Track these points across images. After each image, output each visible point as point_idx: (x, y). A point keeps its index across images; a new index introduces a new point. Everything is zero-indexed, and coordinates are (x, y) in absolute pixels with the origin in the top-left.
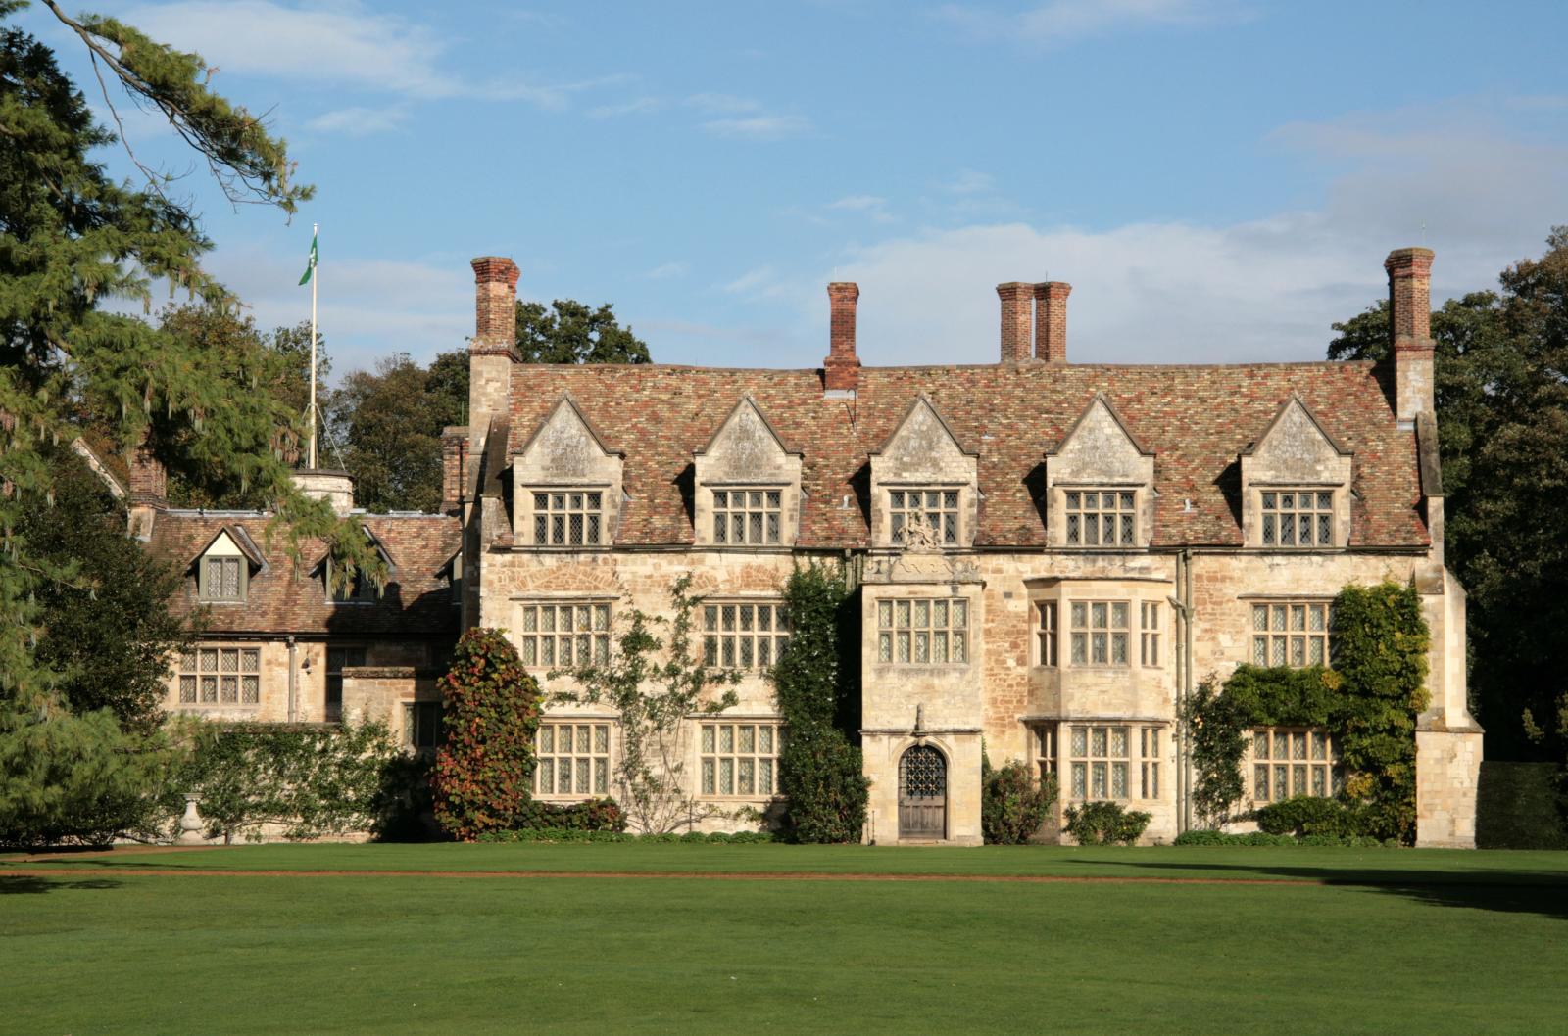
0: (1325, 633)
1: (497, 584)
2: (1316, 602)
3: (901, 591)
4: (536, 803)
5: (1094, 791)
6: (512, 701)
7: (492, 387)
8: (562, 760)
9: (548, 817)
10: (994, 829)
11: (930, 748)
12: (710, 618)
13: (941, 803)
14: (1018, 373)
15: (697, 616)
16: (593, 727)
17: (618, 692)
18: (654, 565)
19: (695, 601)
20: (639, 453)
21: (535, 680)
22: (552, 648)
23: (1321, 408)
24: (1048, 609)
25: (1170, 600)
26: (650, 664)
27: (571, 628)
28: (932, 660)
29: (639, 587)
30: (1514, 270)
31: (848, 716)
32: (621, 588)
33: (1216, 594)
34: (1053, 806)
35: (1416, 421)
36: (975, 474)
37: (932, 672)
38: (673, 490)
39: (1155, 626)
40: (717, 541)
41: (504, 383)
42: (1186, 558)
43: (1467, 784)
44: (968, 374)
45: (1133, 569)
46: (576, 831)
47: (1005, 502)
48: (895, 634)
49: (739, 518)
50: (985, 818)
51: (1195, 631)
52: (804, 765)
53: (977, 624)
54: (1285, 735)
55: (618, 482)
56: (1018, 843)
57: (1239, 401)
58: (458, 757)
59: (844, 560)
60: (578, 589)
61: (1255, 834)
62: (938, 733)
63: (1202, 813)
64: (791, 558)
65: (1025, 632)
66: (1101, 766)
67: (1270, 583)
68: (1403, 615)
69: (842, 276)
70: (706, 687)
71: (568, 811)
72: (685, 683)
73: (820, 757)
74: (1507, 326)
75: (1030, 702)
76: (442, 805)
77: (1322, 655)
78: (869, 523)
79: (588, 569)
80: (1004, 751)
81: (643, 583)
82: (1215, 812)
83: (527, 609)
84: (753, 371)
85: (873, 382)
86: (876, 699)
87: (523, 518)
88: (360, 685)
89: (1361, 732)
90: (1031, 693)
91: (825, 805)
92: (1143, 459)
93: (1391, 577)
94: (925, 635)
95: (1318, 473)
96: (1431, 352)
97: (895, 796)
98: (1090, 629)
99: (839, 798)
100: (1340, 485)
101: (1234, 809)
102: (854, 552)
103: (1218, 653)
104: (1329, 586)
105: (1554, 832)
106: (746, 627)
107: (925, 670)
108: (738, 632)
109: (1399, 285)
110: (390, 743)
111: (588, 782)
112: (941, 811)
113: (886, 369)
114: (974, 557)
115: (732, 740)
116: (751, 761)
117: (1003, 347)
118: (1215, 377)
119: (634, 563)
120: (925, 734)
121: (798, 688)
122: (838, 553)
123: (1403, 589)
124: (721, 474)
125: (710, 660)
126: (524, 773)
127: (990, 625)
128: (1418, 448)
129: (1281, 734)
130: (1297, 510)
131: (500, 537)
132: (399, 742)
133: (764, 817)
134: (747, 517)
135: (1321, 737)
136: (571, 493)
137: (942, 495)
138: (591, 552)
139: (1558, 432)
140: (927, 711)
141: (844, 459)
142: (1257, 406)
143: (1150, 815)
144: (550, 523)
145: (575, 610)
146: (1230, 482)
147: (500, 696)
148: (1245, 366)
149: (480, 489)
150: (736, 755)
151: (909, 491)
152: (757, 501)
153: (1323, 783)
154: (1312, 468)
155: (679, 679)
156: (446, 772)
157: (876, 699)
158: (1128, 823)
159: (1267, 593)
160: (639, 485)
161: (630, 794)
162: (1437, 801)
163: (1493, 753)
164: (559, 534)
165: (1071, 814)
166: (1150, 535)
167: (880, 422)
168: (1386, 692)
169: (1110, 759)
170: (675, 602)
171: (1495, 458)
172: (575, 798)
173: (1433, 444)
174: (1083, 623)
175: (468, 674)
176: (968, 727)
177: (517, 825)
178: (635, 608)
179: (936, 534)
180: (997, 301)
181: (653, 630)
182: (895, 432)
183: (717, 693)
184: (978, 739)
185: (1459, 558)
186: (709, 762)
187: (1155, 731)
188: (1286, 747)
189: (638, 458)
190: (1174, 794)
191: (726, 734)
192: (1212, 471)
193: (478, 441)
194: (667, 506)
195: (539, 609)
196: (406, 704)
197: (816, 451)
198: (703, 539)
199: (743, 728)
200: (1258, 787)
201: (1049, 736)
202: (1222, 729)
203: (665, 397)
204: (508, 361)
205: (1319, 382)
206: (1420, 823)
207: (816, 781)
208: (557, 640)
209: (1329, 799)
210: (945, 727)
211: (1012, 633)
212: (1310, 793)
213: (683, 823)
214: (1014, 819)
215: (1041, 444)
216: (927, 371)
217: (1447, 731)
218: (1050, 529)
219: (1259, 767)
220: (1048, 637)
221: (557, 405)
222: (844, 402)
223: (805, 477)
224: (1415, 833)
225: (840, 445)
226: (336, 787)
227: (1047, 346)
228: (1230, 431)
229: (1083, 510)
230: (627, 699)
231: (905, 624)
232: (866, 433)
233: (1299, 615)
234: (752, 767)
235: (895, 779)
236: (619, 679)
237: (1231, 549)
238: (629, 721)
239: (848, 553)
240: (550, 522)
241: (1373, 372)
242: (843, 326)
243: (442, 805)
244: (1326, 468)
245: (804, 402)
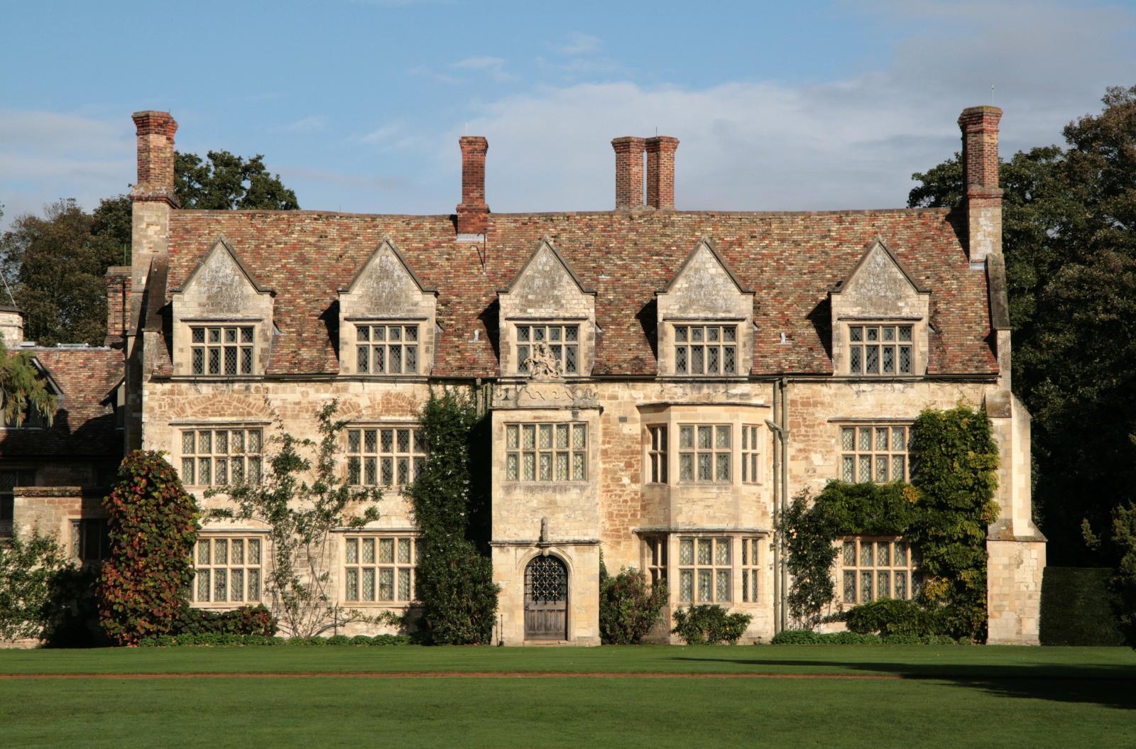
0: (906, 453)
1: (157, 411)
2: (897, 424)
3: (527, 416)
4: (194, 610)
5: (700, 595)
6: (171, 517)
7: (152, 230)
8: (217, 571)
9: (205, 623)
10: (611, 630)
11: (553, 557)
12: (354, 441)
13: (563, 607)
14: (631, 219)
15: (342, 439)
16: (246, 541)
17: (269, 508)
18: (302, 393)
19: (340, 425)
20: (288, 291)
21: (192, 498)
22: (209, 468)
23: (901, 250)
24: (659, 432)
25: (767, 423)
27: (226, 450)
28: (554, 478)
29: (289, 413)
30: (1077, 125)
31: (478, 528)
32: (272, 414)
33: (808, 418)
34: (663, 609)
35: (986, 262)
36: (593, 310)
38: (320, 325)
39: (754, 447)
40: (360, 371)
41: (163, 227)
42: (782, 386)
43: (1032, 587)
44: (586, 219)
45: (735, 395)
46: (231, 635)
47: (621, 336)
48: (521, 454)
49: (379, 350)
50: (602, 621)
51: (790, 452)
52: (439, 574)
53: (596, 444)
54: (870, 544)
55: (269, 317)
56: (632, 642)
57: (829, 244)
58: (121, 569)
59: (475, 388)
60: (232, 415)
61: (843, 634)
62: (560, 544)
63: (797, 615)
64: (427, 386)
65: (638, 453)
66: (706, 573)
67: (857, 408)
68: (975, 436)
69: (471, 131)
70: (350, 503)
71: (224, 617)
72: (331, 500)
73: (453, 567)
74: (1067, 176)
75: (643, 516)
76: (107, 613)
77: (903, 472)
78: (497, 354)
79: (242, 397)
80: (620, 560)
81: (292, 409)
82: (808, 614)
83: (185, 434)
84: (392, 216)
85: (501, 226)
86: (504, 513)
87: (181, 350)
88: (30, 503)
89: (938, 540)
90: (644, 508)
91: (458, 610)
92: (744, 297)
93: (964, 402)
94: (548, 456)
95: (899, 309)
96: (999, 200)
97: (521, 602)
98: (696, 450)
99: (471, 603)
100: (919, 320)
101: (825, 611)
102: (485, 381)
103: (812, 471)
105: (1109, 630)
106: (386, 449)
107: (548, 488)
108: (379, 454)
109: (971, 139)
110: (58, 556)
111: (242, 591)
112: (563, 615)
113: (513, 215)
114: (592, 385)
115: (373, 551)
116: (391, 570)
117: (618, 196)
118: (808, 223)
119: (284, 391)
120: (549, 545)
121: (434, 504)
122: (470, 381)
123: (975, 413)
124: (363, 310)
125: (354, 480)
126: (182, 583)
127: (607, 446)
128: (988, 286)
129: (867, 544)
130: (881, 342)
131: (160, 367)
132: (67, 556)
133: (402, 621)
134: (387, 349)
135: (903, 546)
136: (226, 327)
137: (564, 329)
138: (244, 381)
139: (1112, 271)
140: (550, 525)
141: (475, 296)
142: (845, 249)
143: (750, 617)
144: (207, 354)
145: (230, 434)
146: (821, 317)
147: (161, 512)
148: (834, 213)
149: (142, 324)
150: (378, 564)
151: (534, 326)
152: (396, 335)
153: (904, 587)
154: (894, 304)
155: (326, 496)
156: (110, 583)
157: (504, 513)
158: (730, 625)
160: (288, 320)
161: (281, 601)
162: (1005, 603)
163: (1054, 558)
164: (214, 365)
165: (679, 616)
166: (750, 365)
167: (507, 264)
168: (961, 505)
169: (714, 567)
170: (321, 427)
171: (1057, 295)
172: (230, 605)
173: (1002, 281)
174: (691, 444)
175: (130, 492)
176: (587, 538)
177: (176, 631)
178: (285, 432)
179: (558, 364)
180: (612, 154)
181: (302, 452)
182: (521, 272)
183: (360, 509)
184: (596, 549)
185: (1024, 386)
186: (352, 571)
187: (755, 541)
188: (871, 555)
189: (287, 296)
190: (772, 598)
191: (368, 546)
192: (805, 307)
193: (140, 280)
194: (314, 339)
195: (197, 433)
196: (73, 521)
197: (450, 289)
198: (347, 369)
199: (383, 540)
200: (846, 591)
201: (660, 546)
202: (814, 539)
203: (312, 240)
204: (167, 206)
205: (900, 227)
206: (991, 622)
207: (450, 588)
208: (213, 461)
209: (909, 602)
210: (566, 538)
211: (627, 453)
212: (893, 596)
213: (329, 627)
214: (628, 621)
215: (652, 283)
216: (549, 217)
217: (1014, 540)
218: (660, 360)
219: (847, 573)
220: (659, 457)
221: (213, 247)
222: (475, 245)
223: (439, 313)
224: (986, 631)
225: (471, 284)
226: (7, 598)
227: (658, 195)
228: (822, 271)
229: (690, 342)
230: (278, 515)
231: (530, 446)
232: (495, 273)
233: (883, 436)
234: (392, 576)
235: (522, 585)
236: (270, 497)
237: (822, 377)
238: (280, 535)
239: (479, 381)
240: (207, 354)
241: (948, 218)
242: (473, 176)
243: (107, 613)
244: (907, 304)
245: (438, 245)
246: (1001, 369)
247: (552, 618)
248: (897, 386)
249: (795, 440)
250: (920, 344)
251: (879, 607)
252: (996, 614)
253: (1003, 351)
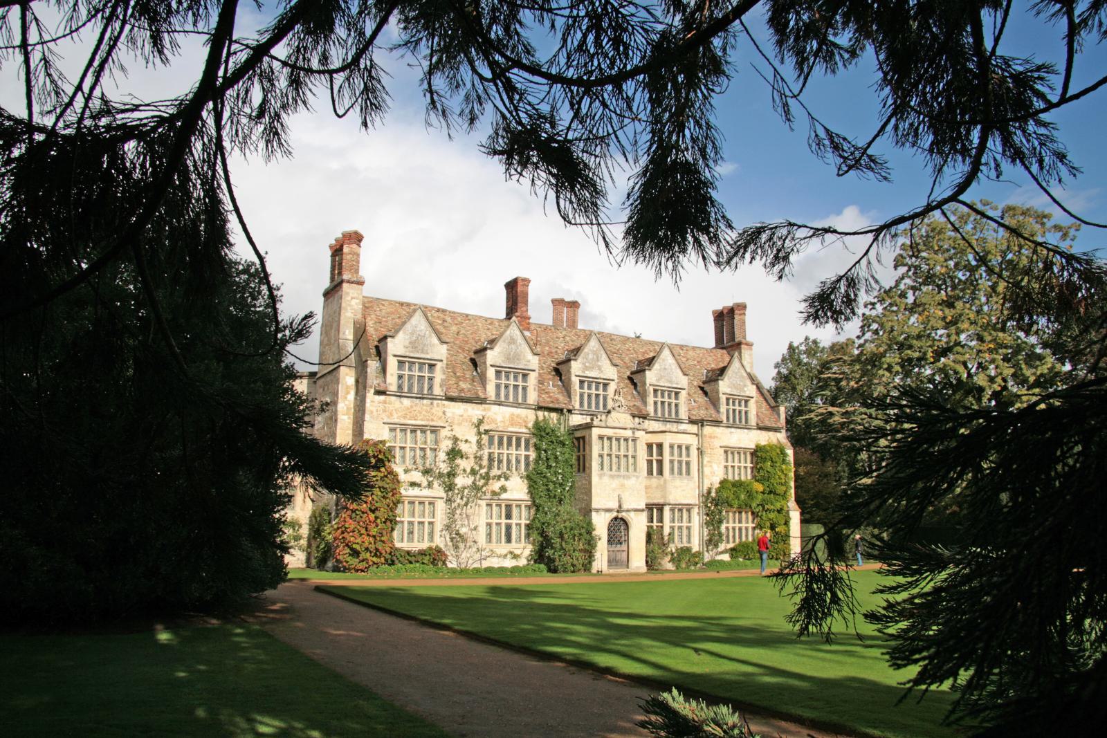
1: (375, 413)
10: (651, 563)
11: (622, 519)
13: (626, 549)
16: (427, 503)
19: (487, 432)
26: (462, 467)
29: (456, 422)
37: (624, 477)
42: (702, 426)
49: (507, 387)
50: (647, 556)
51: (705, 462)
60: (422, 420)
62: (628, 511)
63: (708, 551)
78: (570, 397)
81: (459, 421)
83: (391, 430)
87: (392, 375)
103: (713, 473)
109: (737, 317)
112: (625, 554)
122: (559, 411)
125: (490, 467)
136: (420, 363)
142: (691, 362)
145: (419, 432)
152: (516, 378)
155: (478, 476)
161: (450, 544)
165: (672, 554)
172: (417, 546)
178: (454, 433)
181: (463, 447)
183: (496, 486)
186: (489, 525)
195: (398, 430)
230: (450, 487)
237: (716, 423)
238: (450, 500)
247: (618, 554)
251: (741, 544)
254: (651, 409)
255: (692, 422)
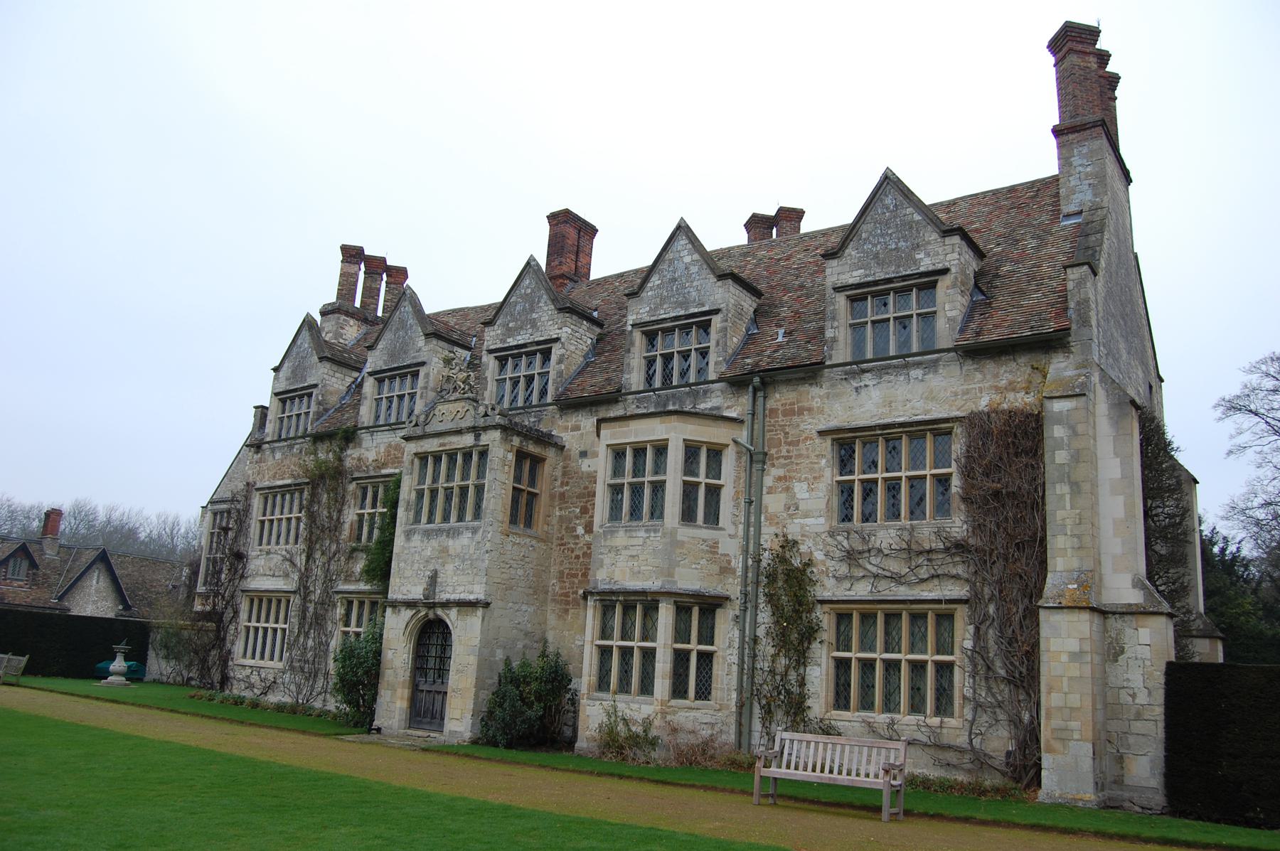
23: (977, 225)
25: (735, 442)
35: (1080, 212)
51: (768, 481)
62: (447, 605)
86: (402, 565)
92: (720, 283)
95: (916, 262)
100: (945, 271)
103: (793, 508)
104: (930, 405)
159: (854, 424)
162: (1074, 724)
176: (472, 597)
184: (480, 612)
190: (734, 695)
237: (810, 372)
246: (1074, 327)
248: (916, 373)
249: (773, 465)
250: (947, 307)
252: (1057, 745)
253: (1077, 298)
254: (635, 378)
255: (737, 383)
